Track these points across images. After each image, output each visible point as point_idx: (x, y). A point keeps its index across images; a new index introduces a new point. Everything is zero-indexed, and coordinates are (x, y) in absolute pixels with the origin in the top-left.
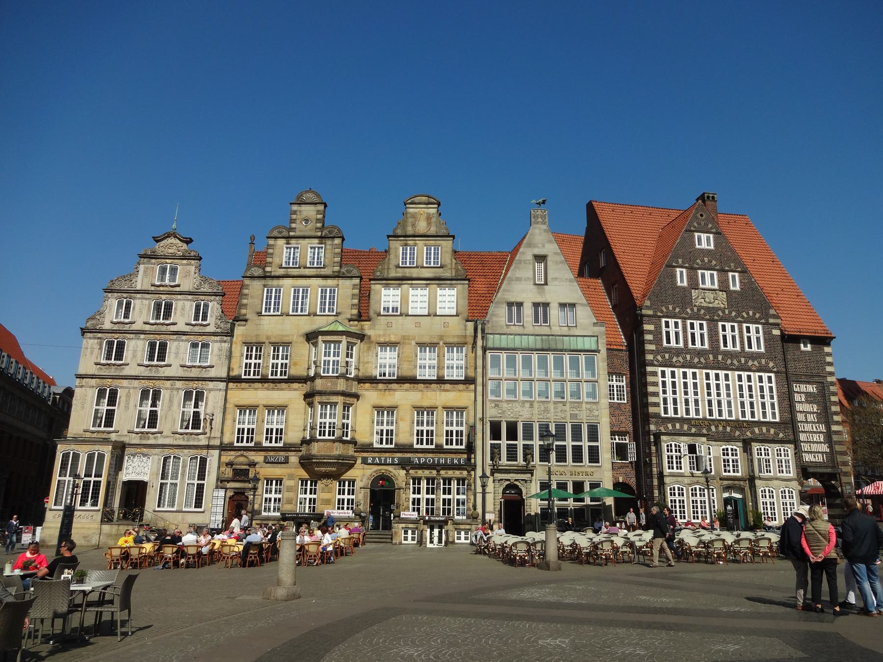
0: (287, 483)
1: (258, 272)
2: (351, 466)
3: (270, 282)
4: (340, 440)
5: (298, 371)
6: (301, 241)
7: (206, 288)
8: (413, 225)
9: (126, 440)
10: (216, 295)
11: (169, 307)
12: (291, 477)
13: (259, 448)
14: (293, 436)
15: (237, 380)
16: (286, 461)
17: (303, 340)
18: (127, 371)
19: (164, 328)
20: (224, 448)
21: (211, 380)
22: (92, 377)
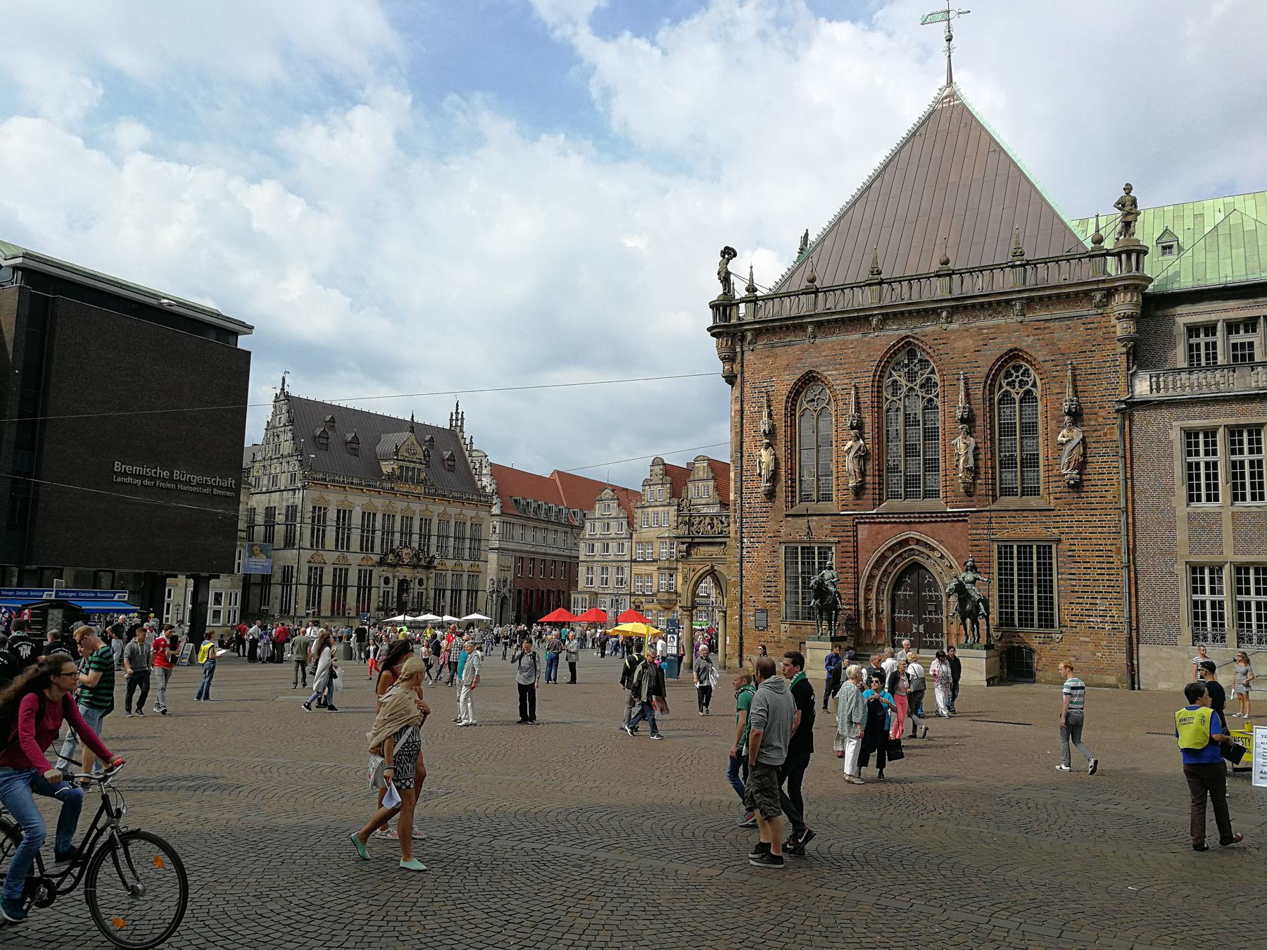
0: (654, 612)
1: (639, 505)
2: (675, 604)
3: (644, 510)
4: (667, 592)
5: (655, 556)
6: (656, 487)
7: (621, 515)
8: (698, 473)
9: (597, 591)
10: (624, 518)
11: (608, 524)
12: (655, 609)
13: (644, 595)
14: (655, 589)
15: (635, 561)
16: (653, 601)
17: (656, 540)
18: (596, 559)
19: (607, 536)
20: (631, 595)
21: (626, 561)
22: (584, 562)
